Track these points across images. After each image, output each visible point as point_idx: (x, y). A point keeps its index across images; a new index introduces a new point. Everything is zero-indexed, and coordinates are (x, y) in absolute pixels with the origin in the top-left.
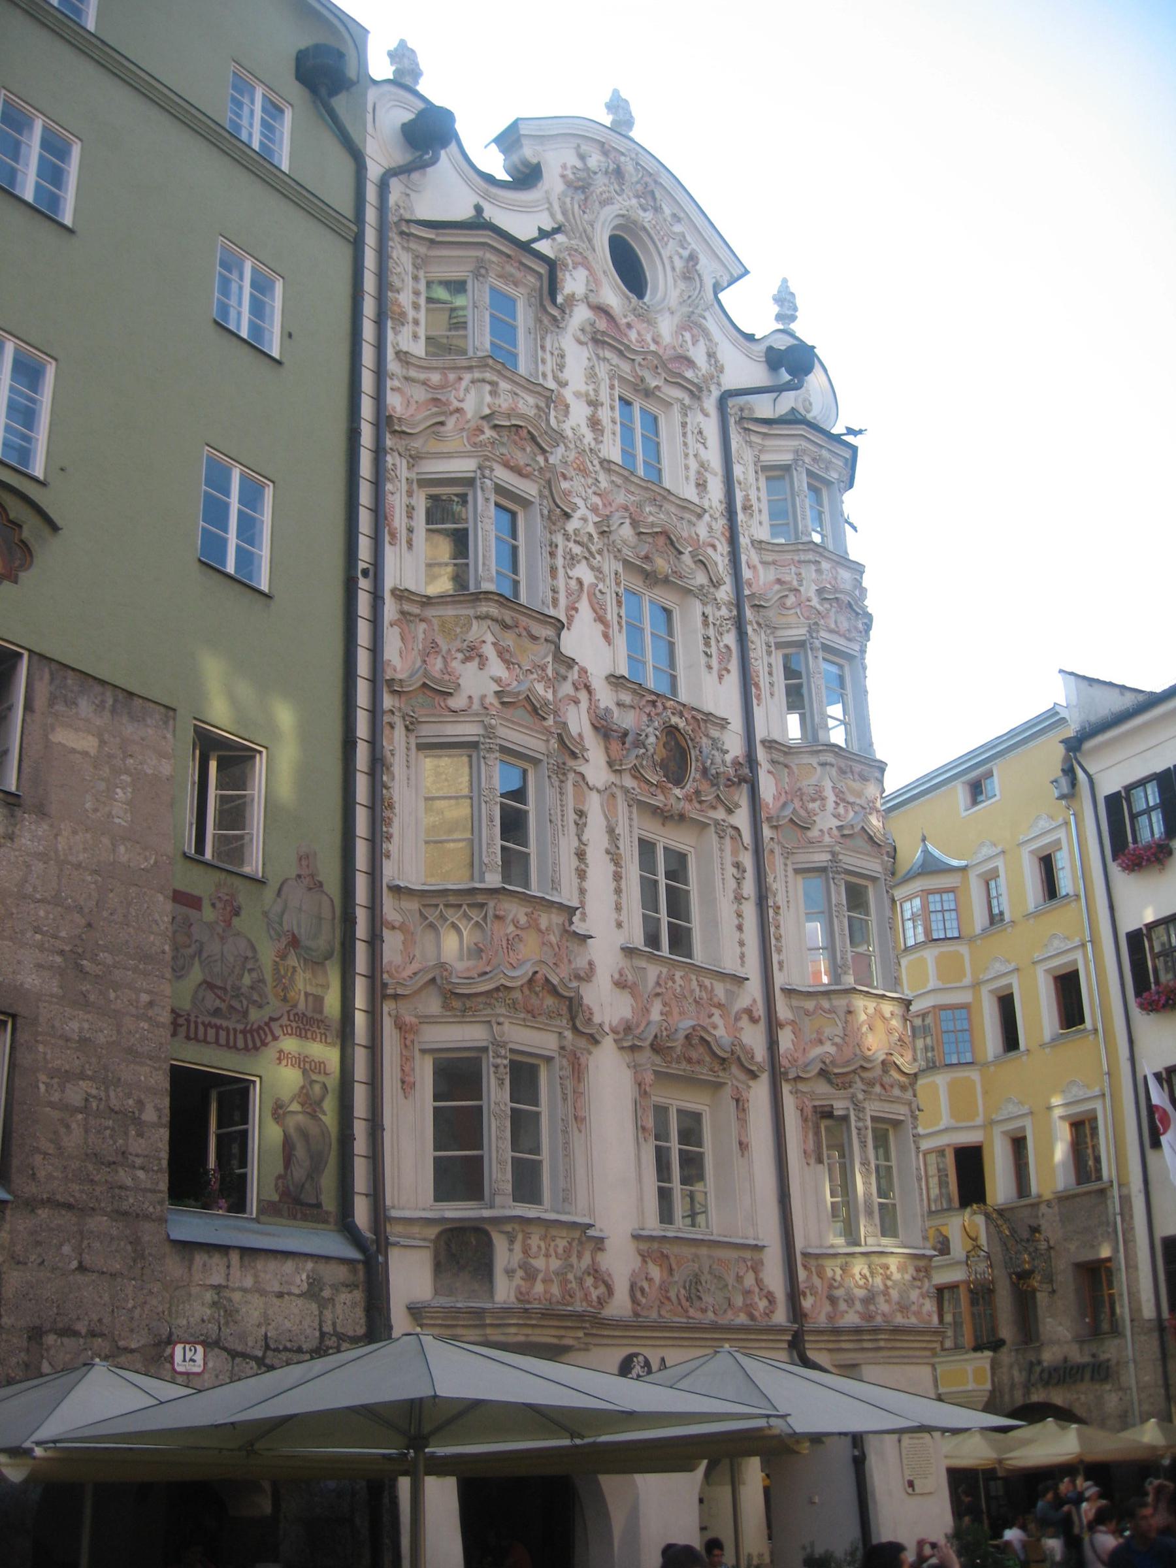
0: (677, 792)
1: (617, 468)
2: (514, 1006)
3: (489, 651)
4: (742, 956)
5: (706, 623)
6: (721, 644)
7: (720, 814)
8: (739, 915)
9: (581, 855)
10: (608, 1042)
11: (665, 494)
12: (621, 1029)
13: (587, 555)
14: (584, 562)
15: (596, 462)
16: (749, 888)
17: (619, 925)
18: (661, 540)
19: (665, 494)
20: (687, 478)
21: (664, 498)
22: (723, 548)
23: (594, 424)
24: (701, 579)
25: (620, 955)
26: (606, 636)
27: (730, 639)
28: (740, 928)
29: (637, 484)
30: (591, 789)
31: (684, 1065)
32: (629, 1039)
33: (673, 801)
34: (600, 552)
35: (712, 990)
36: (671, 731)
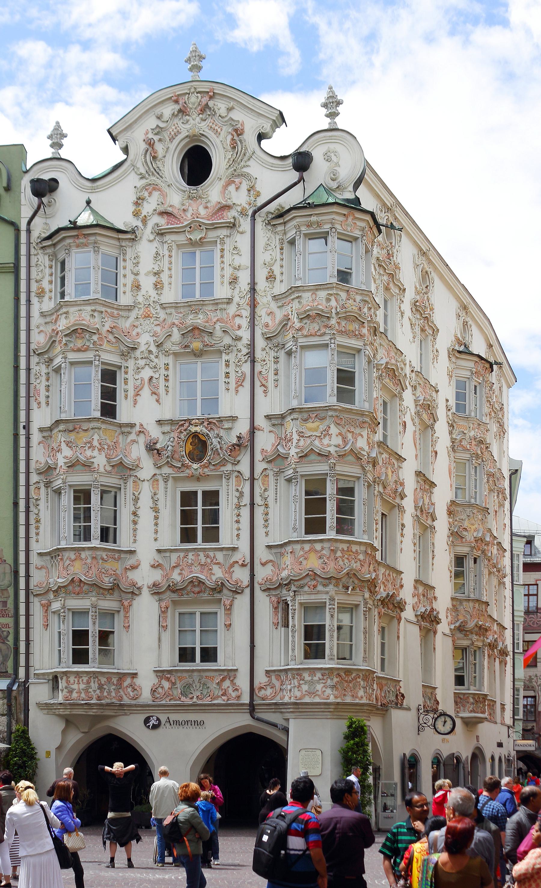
0: (195, 466)
1: (167, 305)
2: (68, 593)
3: (63, 445)
4: (238, 535)
5: (227, 366)
6: (240, 372)
7: (229, 467)
8: (239, 515)
9: (135, 514)
10: (145, 592)
11: (201, 303)
12: (151, 586)
13: (148, 362)
14: (147, 366)
15: (158, 307)
16: (246, 500)
17: (156, 540)
18: (197, 332)
19: (201, 303)
20: (222, 283)
21: (203, 305)
22: (246, 313)
23: (158, 286)
24: (227, 340)
25: (155, 553)
26: (157, 401)
27: (246, 368)
28: (238, 522)
29: (183, 306)
30: (144, 480)
31: (192, 595)
32: (156, 590)
33: (193, 471)
34: (157, 357)
35: (214, 557)
36: (195, 435)
